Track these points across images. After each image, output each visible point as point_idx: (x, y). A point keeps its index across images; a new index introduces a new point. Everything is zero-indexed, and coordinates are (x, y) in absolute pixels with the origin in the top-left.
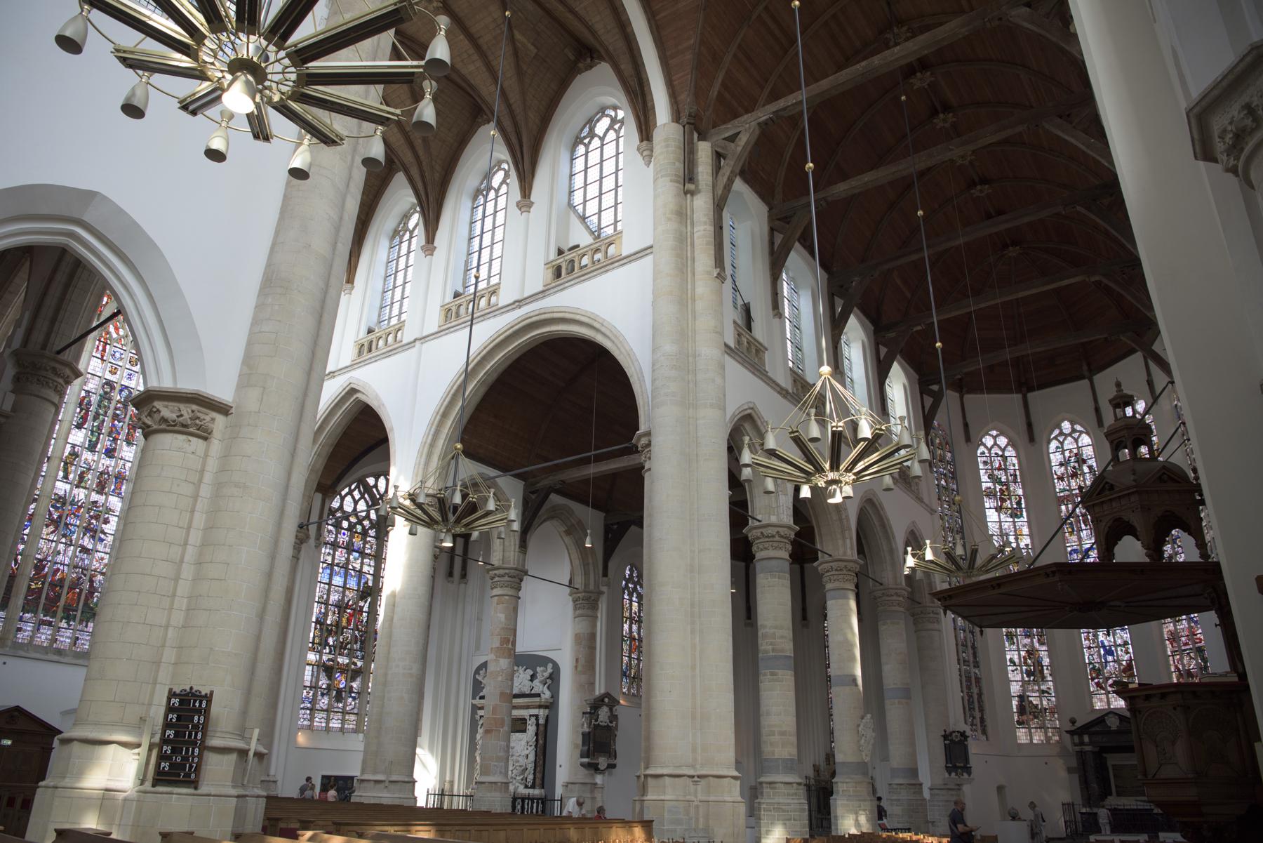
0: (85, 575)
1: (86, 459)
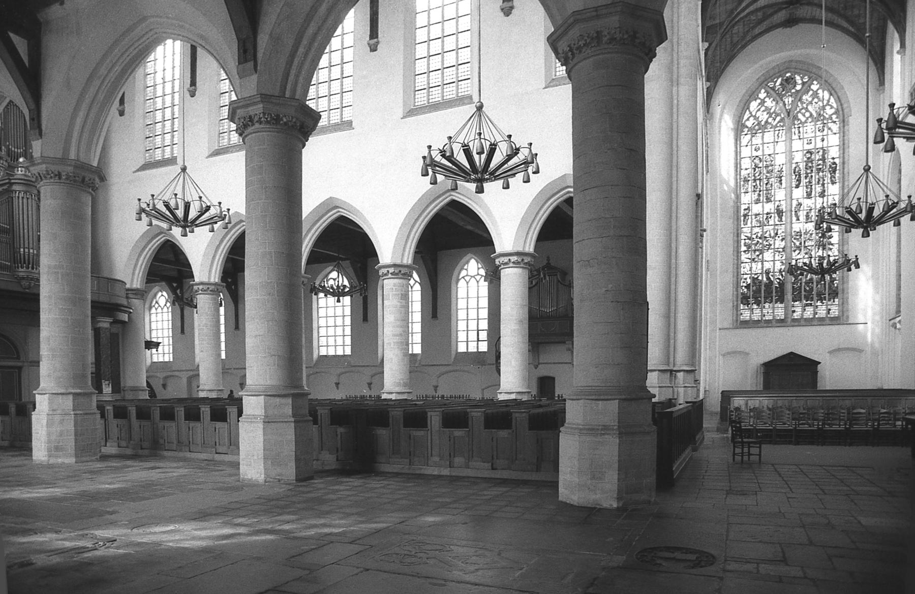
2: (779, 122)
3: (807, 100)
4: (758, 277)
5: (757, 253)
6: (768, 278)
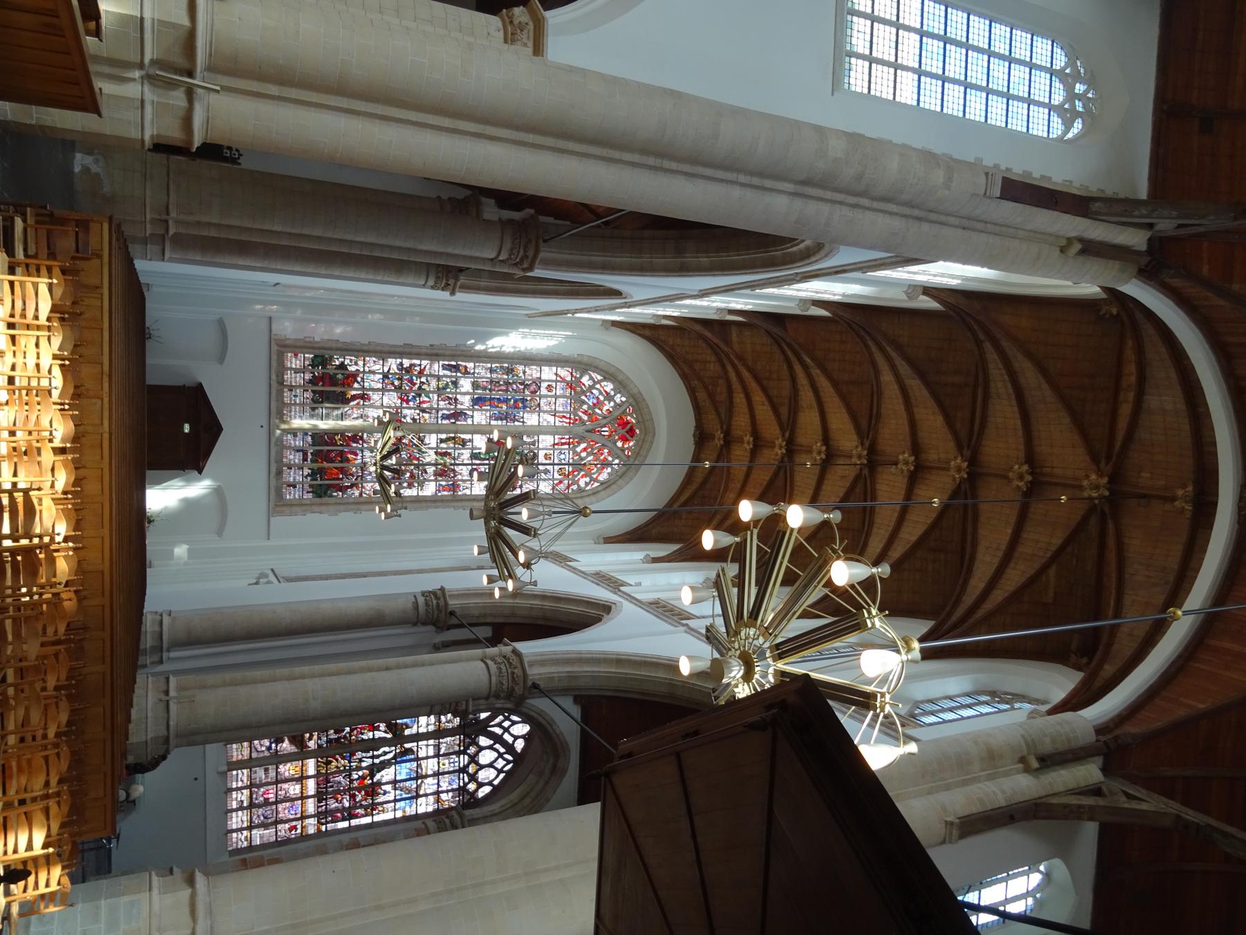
0: (356, 479)
1: (462, 454)
2: (581, 418)
3: (602, 454)
4: (358, 383)
5: (396, 383)
6: (354, 397)
